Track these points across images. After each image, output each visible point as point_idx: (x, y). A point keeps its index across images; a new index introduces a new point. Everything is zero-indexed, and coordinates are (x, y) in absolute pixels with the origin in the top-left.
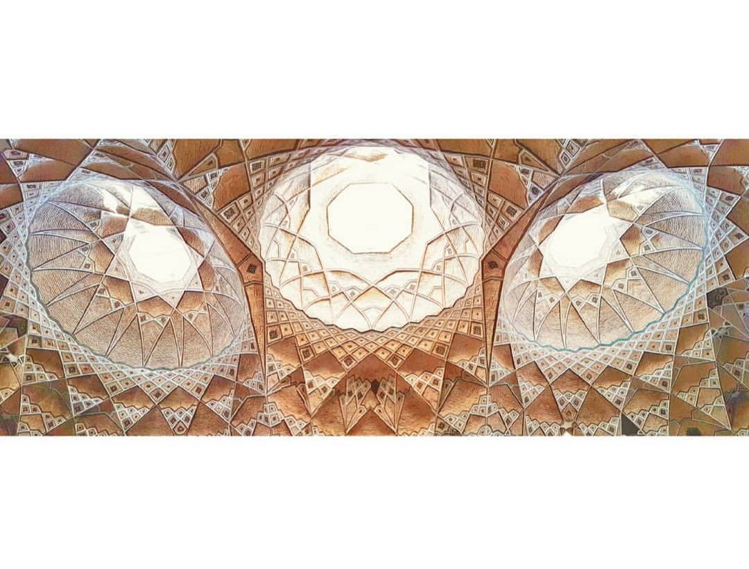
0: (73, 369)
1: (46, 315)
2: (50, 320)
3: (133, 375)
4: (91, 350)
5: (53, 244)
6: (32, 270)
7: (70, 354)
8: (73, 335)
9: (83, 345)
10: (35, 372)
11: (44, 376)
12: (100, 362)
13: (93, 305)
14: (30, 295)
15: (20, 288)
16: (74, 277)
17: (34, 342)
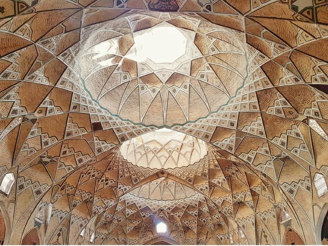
0: (184, 207)
1: (164, 202)
2: (166, 202)
3: (196, 198)
4: (182, 199)
5: (144, 190)
6: (149, 199)
7: (179, 204)
8: (175, 199)
9: (180, 199)
10: (178, 214)
11: (181, 214)
12: (187, 200)
13: (170, 188)
14: (156, 202)
15: (152, 204)
16: (158, 188)
17: (169, 209)
